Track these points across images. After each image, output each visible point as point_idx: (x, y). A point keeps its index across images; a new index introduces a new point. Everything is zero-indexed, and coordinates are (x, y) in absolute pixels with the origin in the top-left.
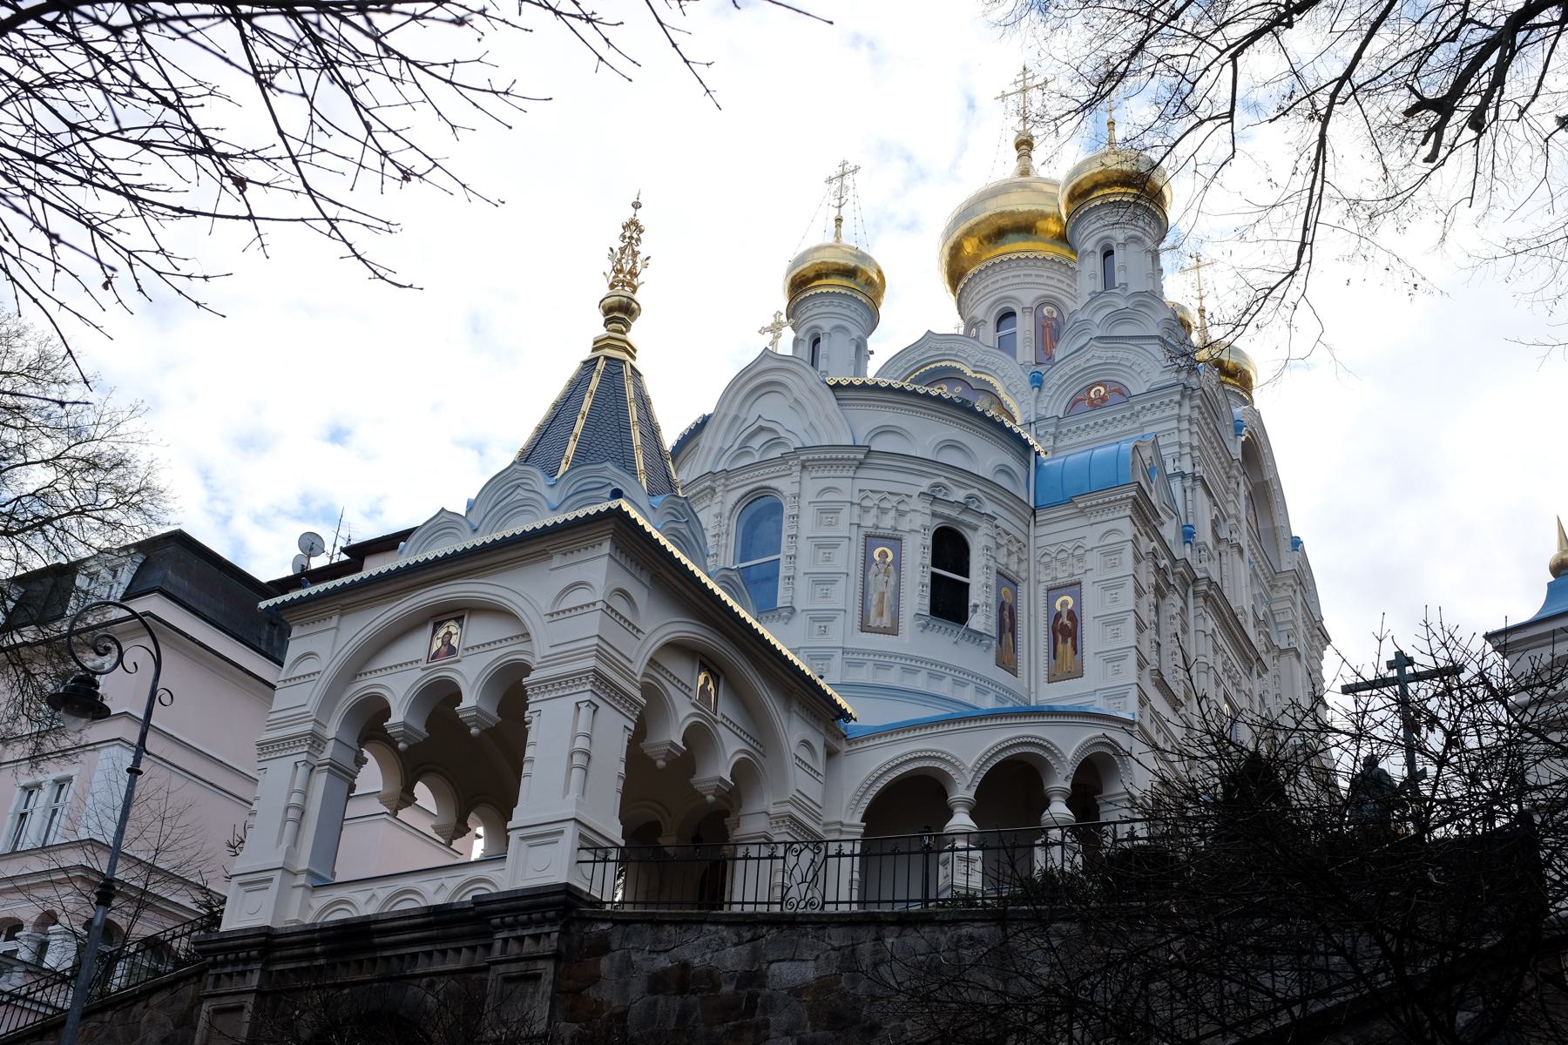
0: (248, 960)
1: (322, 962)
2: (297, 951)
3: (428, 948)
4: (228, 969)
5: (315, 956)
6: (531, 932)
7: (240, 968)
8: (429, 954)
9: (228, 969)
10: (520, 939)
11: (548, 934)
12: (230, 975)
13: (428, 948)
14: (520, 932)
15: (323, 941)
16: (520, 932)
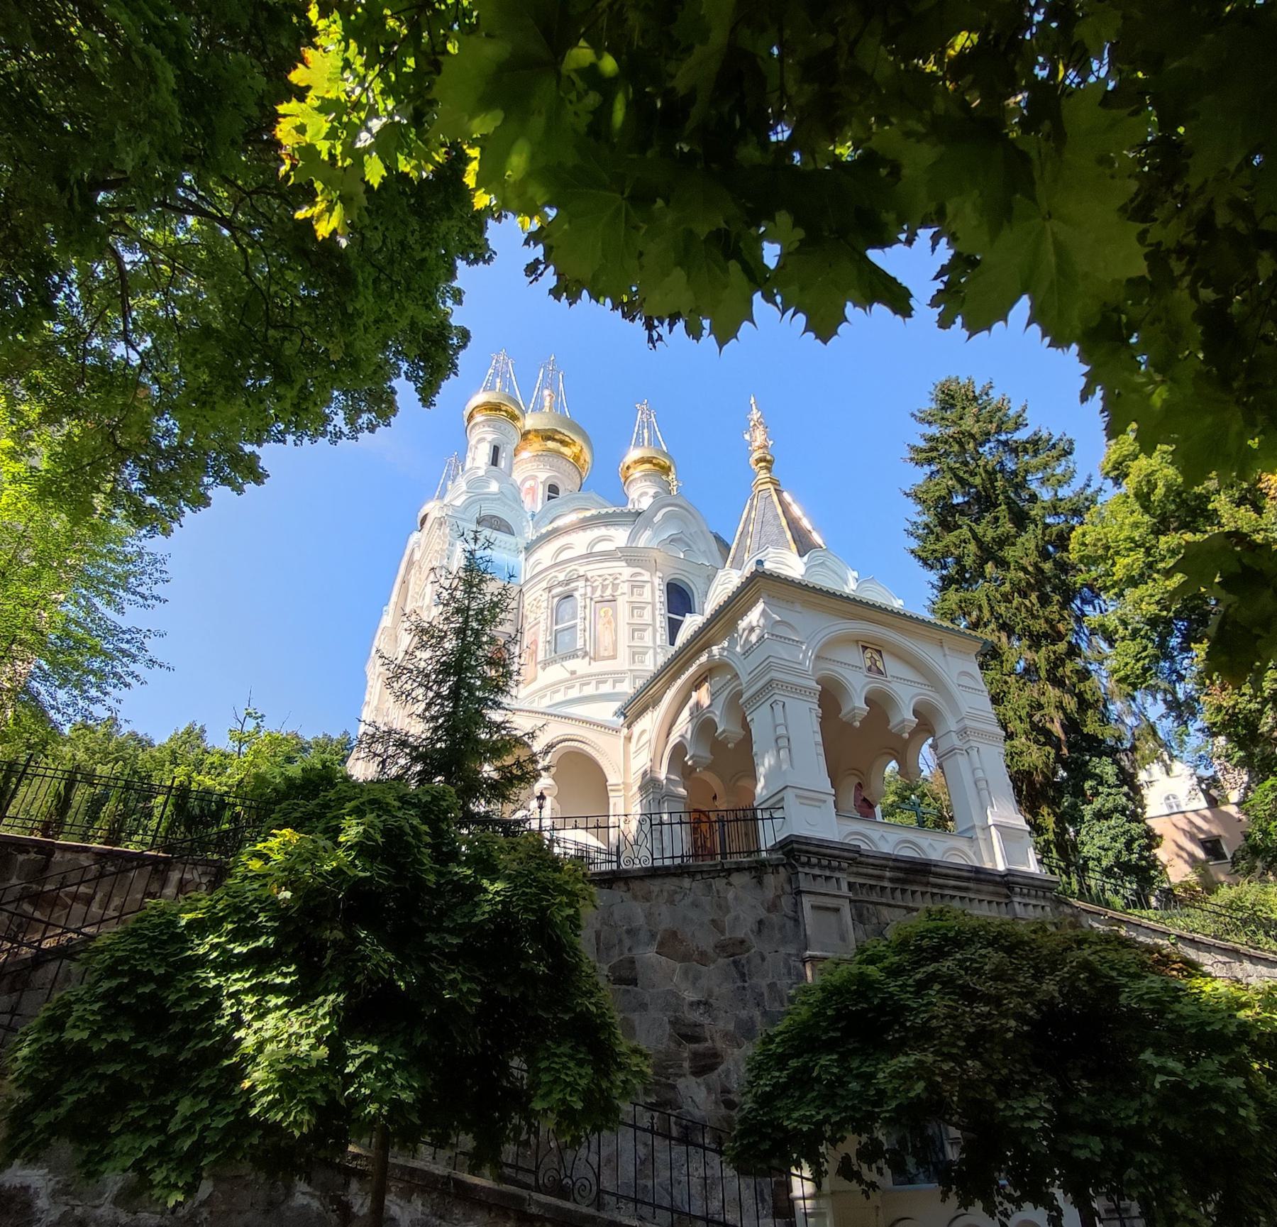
0: (840, 869)
1: (886, 884)
2: (870, 871)
3: (963, 894)
4: (817, 871)
5: (881, 878)
6: (1034, 902)
7: (828, 873)
8: (962, 898)
9: (817, 871)
10: (1026, 905)
11: (1043, 907)
12: (815, 877)
13: (963, 894)
14: (1027, 901)
15: (892, 869)
16: (1027, 901)
